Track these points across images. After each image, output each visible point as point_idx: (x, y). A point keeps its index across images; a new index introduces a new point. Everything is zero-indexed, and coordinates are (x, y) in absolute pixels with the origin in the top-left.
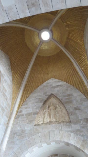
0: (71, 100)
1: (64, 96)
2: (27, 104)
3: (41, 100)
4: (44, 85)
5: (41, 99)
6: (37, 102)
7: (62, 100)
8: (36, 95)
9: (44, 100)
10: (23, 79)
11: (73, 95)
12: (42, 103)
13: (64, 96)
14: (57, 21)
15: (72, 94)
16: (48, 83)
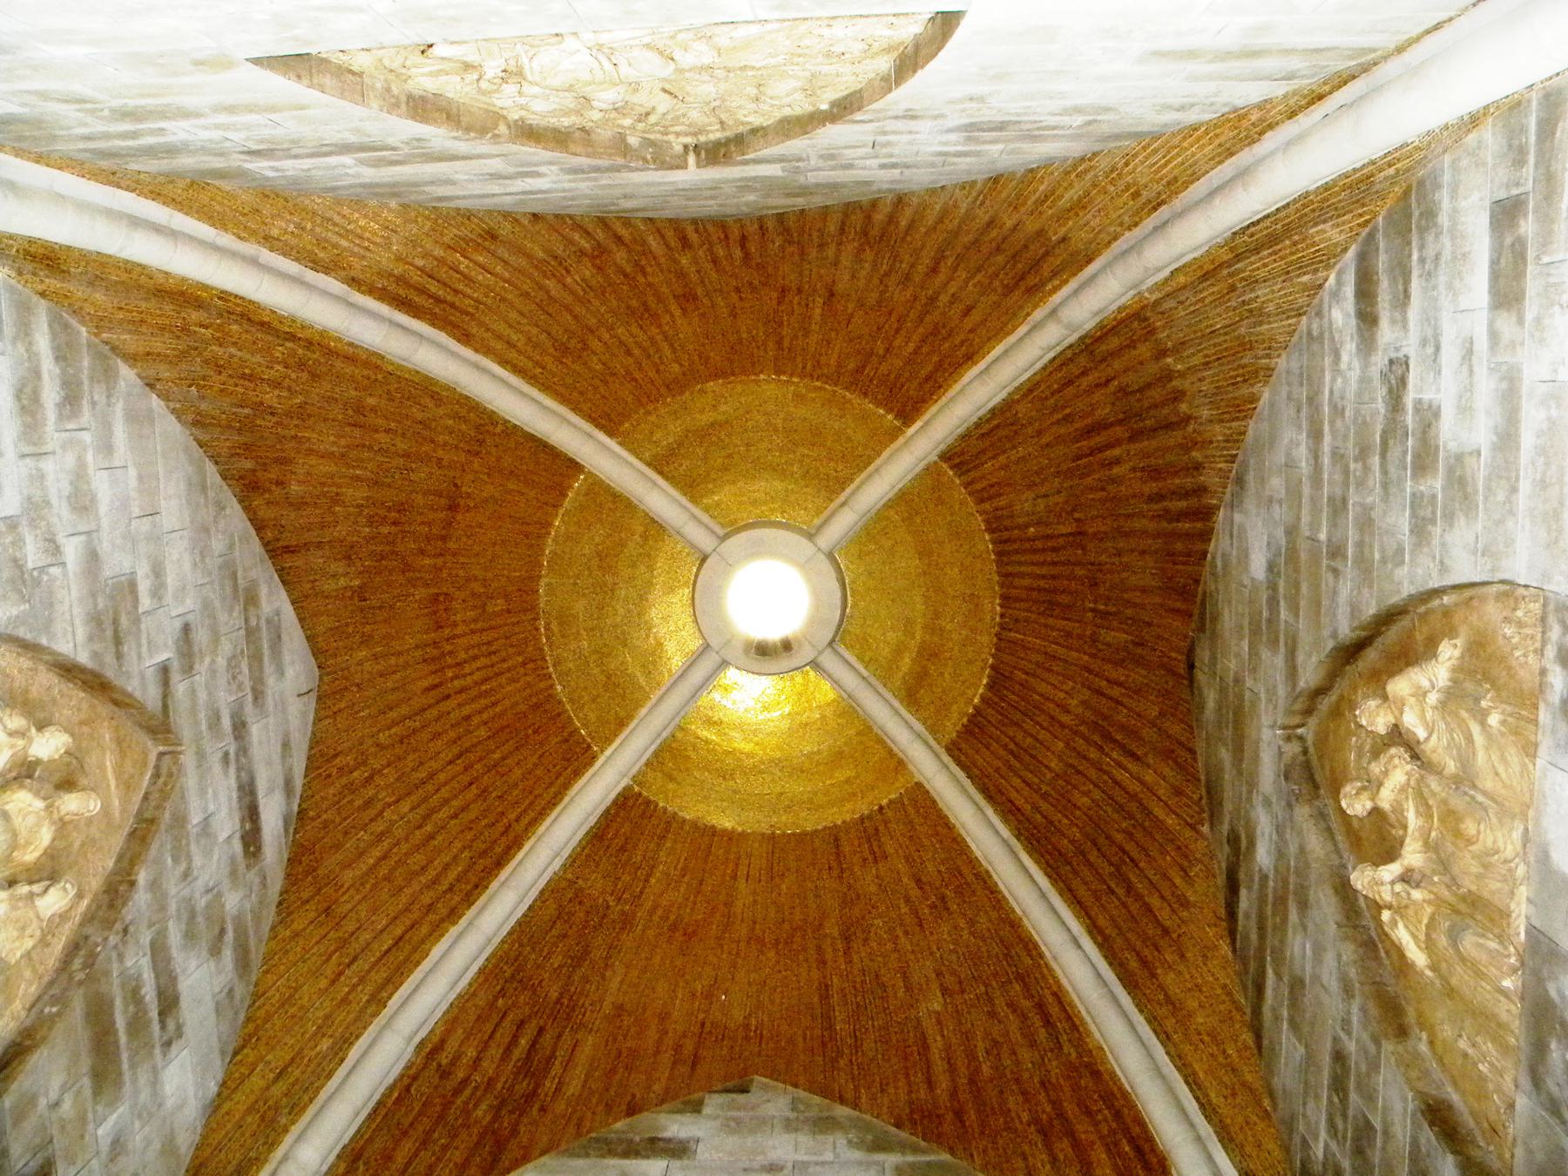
0: (125, 1056)
1: (158, 950)
2: (71, 400)
3: (116, 622)
4: (263, 591)
5: (124, 621)
6: (93, 558)
7: (125, 931)
8: (173, 510)
9: (119, 656)
10: (382, 295)
11: (174, 1048)
12: (83, 658)
13: (158, 950)
14: (900, 765)
15: (179, 1029)
16: (277, 640)
